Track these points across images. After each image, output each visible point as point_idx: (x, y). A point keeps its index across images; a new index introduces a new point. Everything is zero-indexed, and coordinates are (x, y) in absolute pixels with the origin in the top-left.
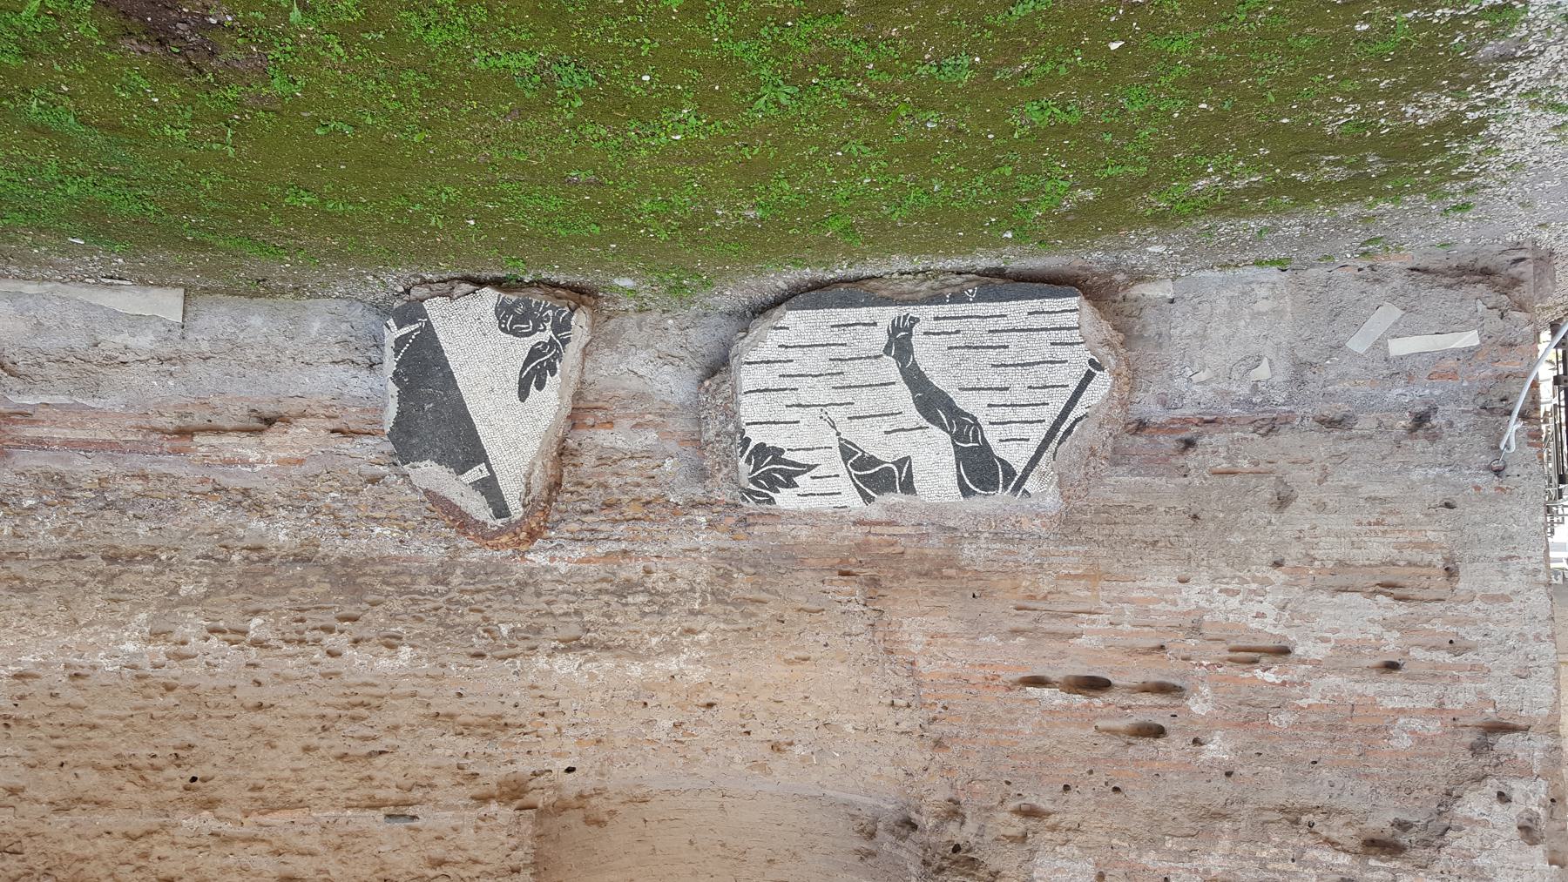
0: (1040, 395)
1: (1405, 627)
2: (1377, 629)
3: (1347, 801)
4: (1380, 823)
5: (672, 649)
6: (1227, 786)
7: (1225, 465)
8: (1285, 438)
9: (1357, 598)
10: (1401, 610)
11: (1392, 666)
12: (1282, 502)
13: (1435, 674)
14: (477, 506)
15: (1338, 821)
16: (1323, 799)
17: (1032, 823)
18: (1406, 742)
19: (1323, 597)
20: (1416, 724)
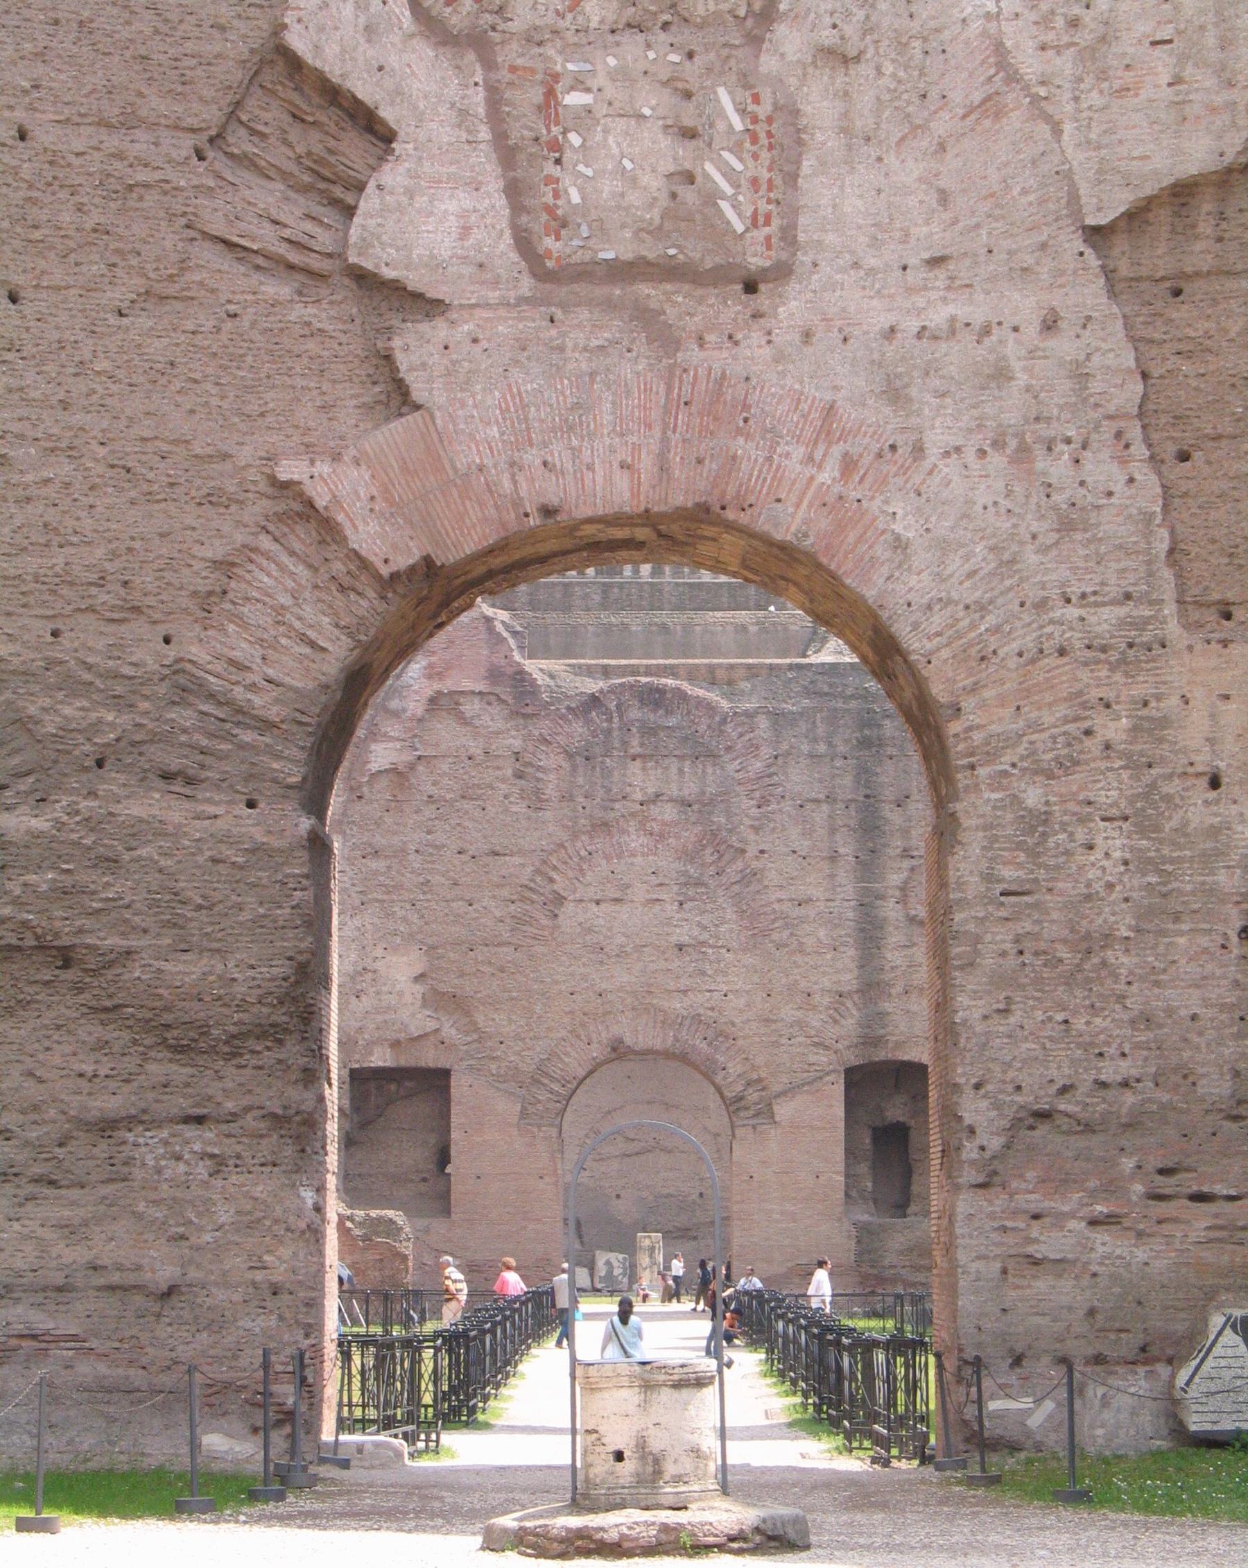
0: (1214, 1374)
1: (1030, 1241)
2: (1042, 1238)
3: (1059, 1139)
4: (1043, 1129)
6: (1124, 1143)
7: (1123, 1335)
8: (1090, 1351)
9: (1052, 1256)
10: (1030, 1249)
11: (1036, 1217)
12: (1092, 1312)
13: (1015, 1213)
15: (1065, 1128)
16: (1073, 1138)
17: (1235, 1112)
18: (1030, 1175)
19: (1070, 1256)
20: (1024, 1185)
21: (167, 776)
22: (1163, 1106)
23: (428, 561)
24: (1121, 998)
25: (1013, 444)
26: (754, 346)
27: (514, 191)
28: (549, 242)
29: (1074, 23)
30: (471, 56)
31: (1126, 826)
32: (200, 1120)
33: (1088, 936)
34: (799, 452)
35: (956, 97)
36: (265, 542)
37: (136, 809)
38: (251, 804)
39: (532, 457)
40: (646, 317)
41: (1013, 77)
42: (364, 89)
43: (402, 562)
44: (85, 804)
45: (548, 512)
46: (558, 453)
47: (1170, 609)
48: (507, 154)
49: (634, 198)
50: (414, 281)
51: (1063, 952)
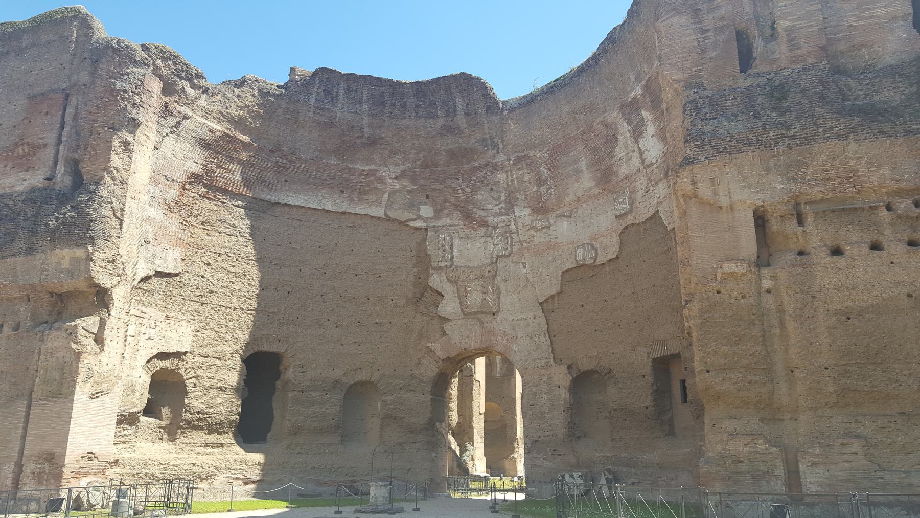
4: (537, 443)
5: (599, 456)
14: (606, 473)
21: (411, 391)
22: (554, 440)
23: (448, 357)
24: (547, 422)
25: (530, 336)
26: (494, 323)
27: (460, 303)
28: (465, 310)
29: (537, 273)
30: (454, 284)
31: (547, 394)
32: (415, 443)
33: (542, 412)
34: (500, 338)
35: (521, 285)
36: (426, 355)
37: (406, 396)
38: (423, 394)
39: (463, 341)
40: (479, 320)
41: (529, 281)
42: (439, 290)
43: (444, 358)
44: (398, 395)
45: (465, 349)
46: (467, 341)
47: (552, 360)
48: (460, 298)
49: (477, 303)
50: (447, 317)
51: (538, 414)
